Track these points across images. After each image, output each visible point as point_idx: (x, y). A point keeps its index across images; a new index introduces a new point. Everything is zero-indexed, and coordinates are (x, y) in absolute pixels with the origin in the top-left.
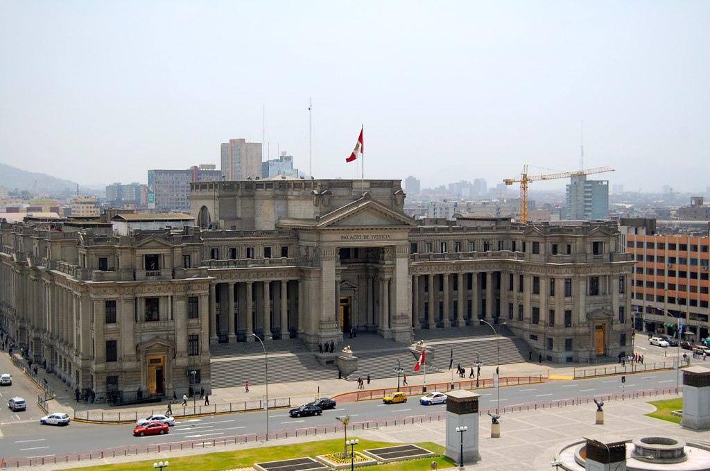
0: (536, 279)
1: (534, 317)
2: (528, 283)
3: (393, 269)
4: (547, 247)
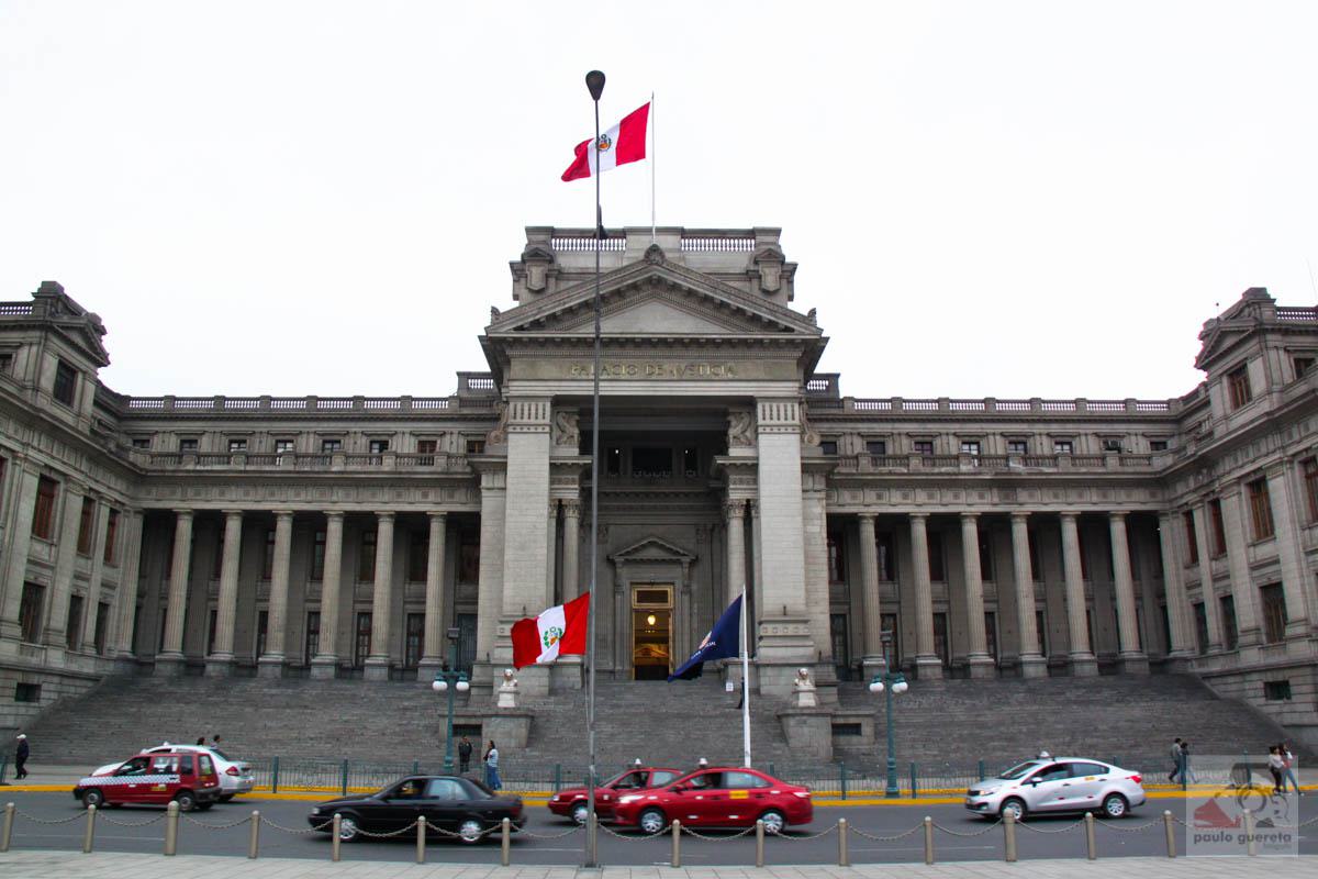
0: (1258, 486)
1: (1268, 619)
2: (1237, 510)
3: (751, 469)
4: (1274, 366)
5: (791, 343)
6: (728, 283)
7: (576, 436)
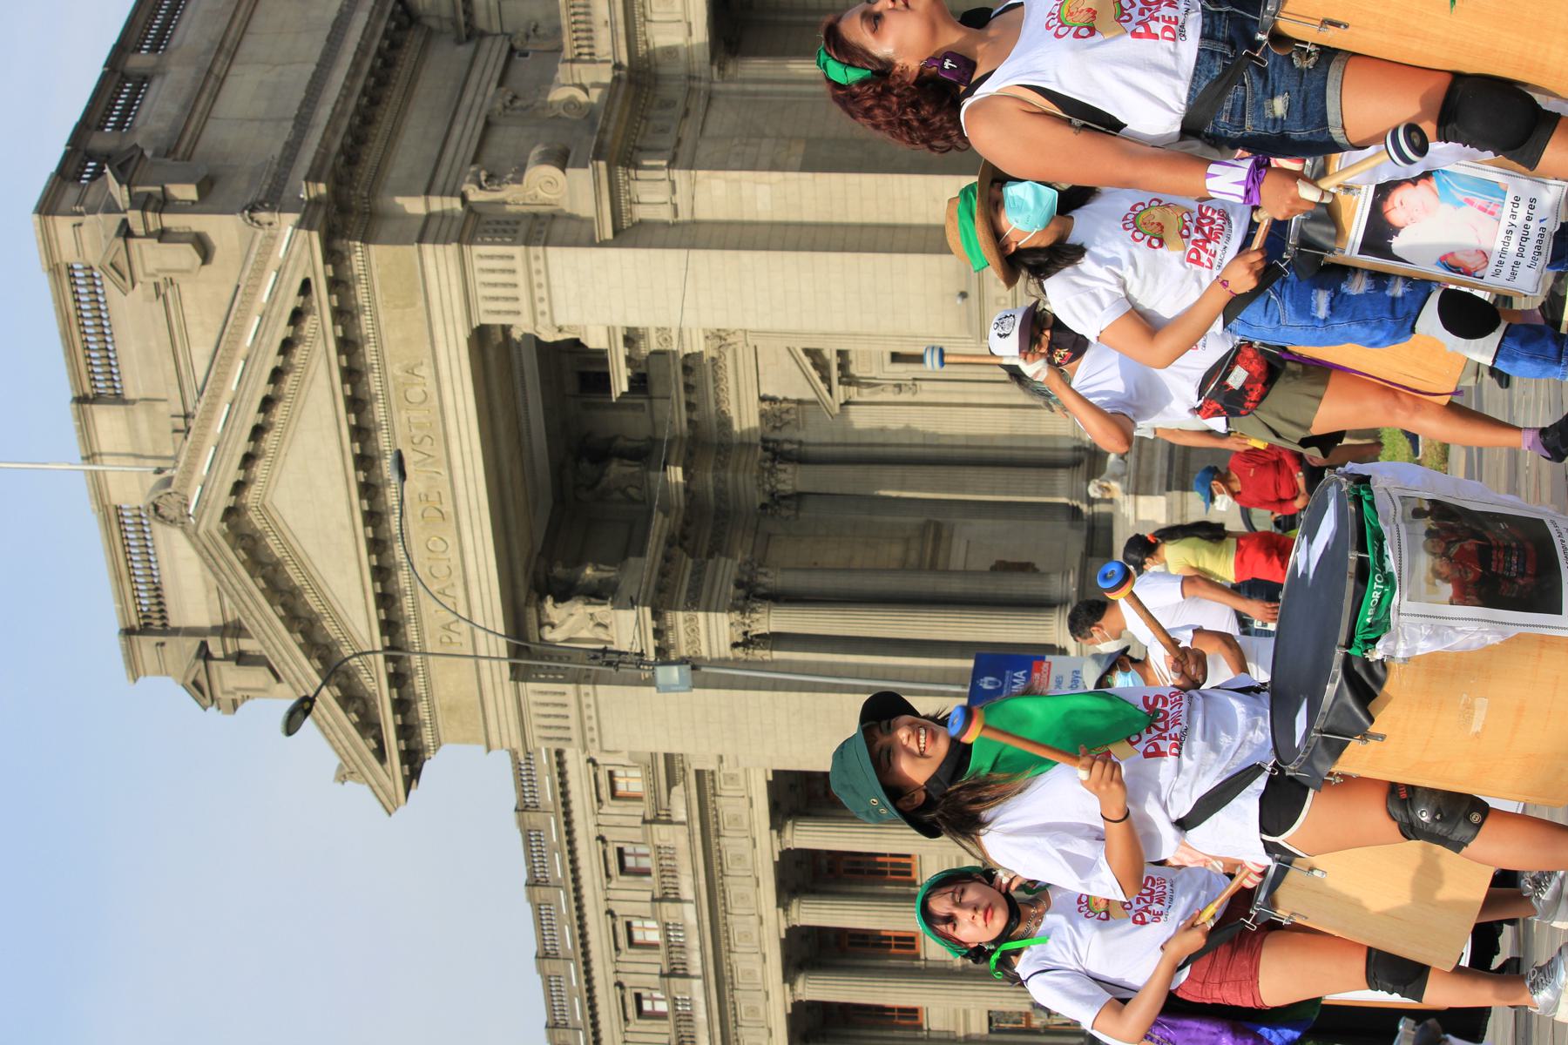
5: (338, 284)
6: (200, 375)
7: (590, 609)
